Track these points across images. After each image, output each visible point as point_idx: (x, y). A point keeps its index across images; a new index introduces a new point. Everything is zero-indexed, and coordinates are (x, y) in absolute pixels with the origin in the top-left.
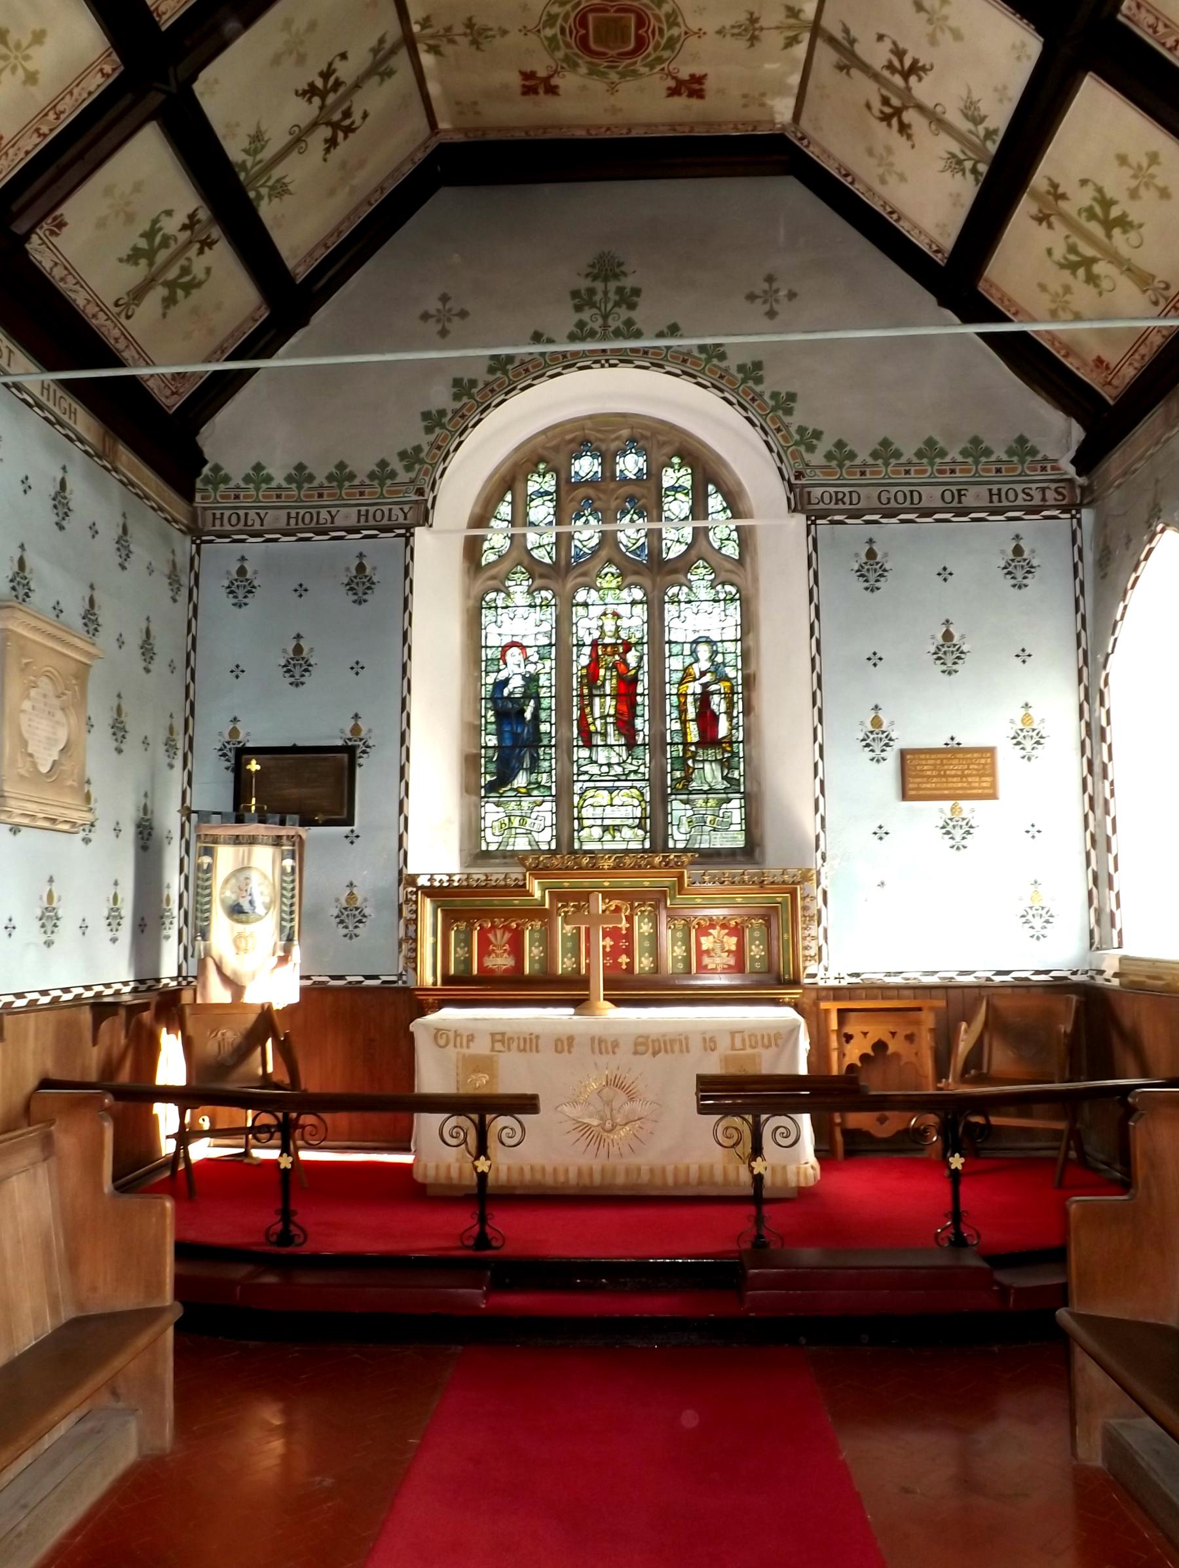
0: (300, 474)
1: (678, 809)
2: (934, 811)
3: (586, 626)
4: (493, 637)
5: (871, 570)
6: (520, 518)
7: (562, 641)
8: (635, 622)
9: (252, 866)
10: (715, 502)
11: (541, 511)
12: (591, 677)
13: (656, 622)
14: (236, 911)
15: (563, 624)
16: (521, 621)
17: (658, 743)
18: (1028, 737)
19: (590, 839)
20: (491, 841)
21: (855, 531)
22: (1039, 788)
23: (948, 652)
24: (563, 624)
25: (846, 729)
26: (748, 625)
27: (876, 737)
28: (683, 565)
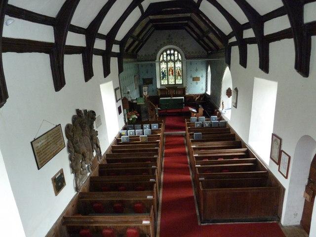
0: (146, 55)
1: (177, 81)
2: (195, 82)
3: (169, 66)
4: (161, 67)
5: (191, 64)
6: (163, 57)
7: (167, 68)
8: (173, 66)
9: (145, 88)
10: (179, 55)
11: (165, 56)
12: (170, 70)
13: (175, 66)
14: (145, 92)
15: (167, 66)
16: (163, 66)
17: (175, 76)
18: (202, 76)
19: (170, 83)
20: (162, 84)
21: (190, 61)
22: (203, 80)
23: (197, 70)
24: (167, 66)
25: (189, 76)
26: (182, 66)
27: (191, 77)
28: (177, 61)
